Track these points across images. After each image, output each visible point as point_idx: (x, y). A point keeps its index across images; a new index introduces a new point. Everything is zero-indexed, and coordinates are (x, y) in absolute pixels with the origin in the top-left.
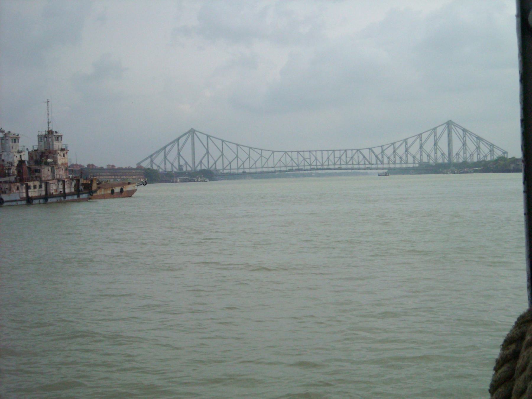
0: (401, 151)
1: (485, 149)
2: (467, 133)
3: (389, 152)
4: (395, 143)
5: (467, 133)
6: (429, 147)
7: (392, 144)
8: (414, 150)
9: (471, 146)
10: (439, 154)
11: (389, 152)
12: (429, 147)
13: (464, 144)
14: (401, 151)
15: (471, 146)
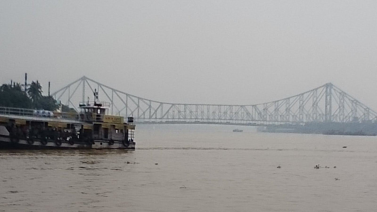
0: (282, 109)
1: (360, 113)
2: (345, 98)
3: (271, 109)
4: (278, 101)
5: (345, 98)
6: (308, 106)
7: (275, 102)
8: (295, 109)
9: (348, 109)
10: (318, 114)
11: (271, 109)
12: (308, 106)
13: (341, 107)
14: (282, 109)
15: (348, 109)
